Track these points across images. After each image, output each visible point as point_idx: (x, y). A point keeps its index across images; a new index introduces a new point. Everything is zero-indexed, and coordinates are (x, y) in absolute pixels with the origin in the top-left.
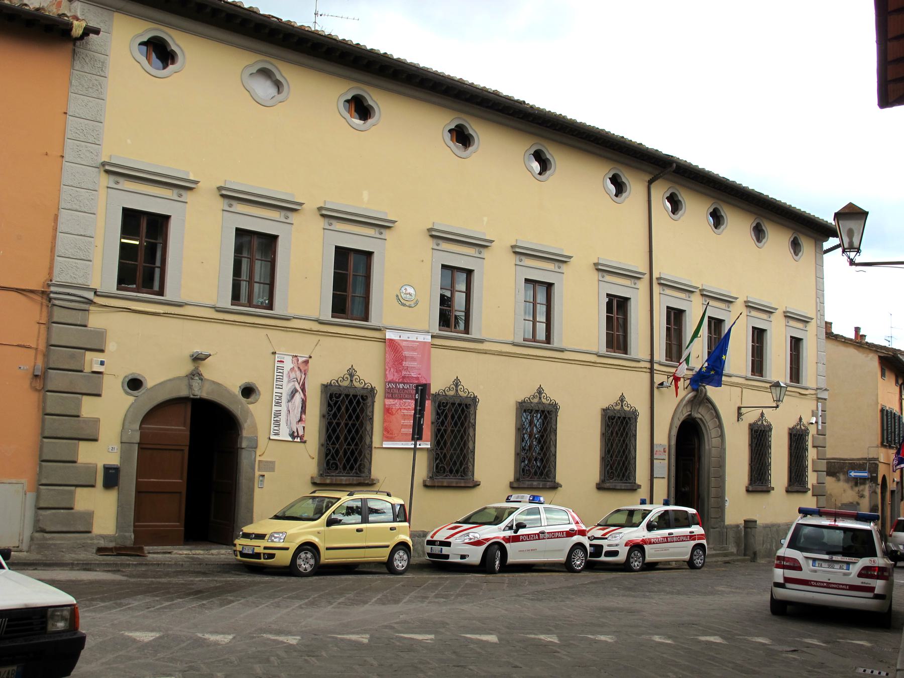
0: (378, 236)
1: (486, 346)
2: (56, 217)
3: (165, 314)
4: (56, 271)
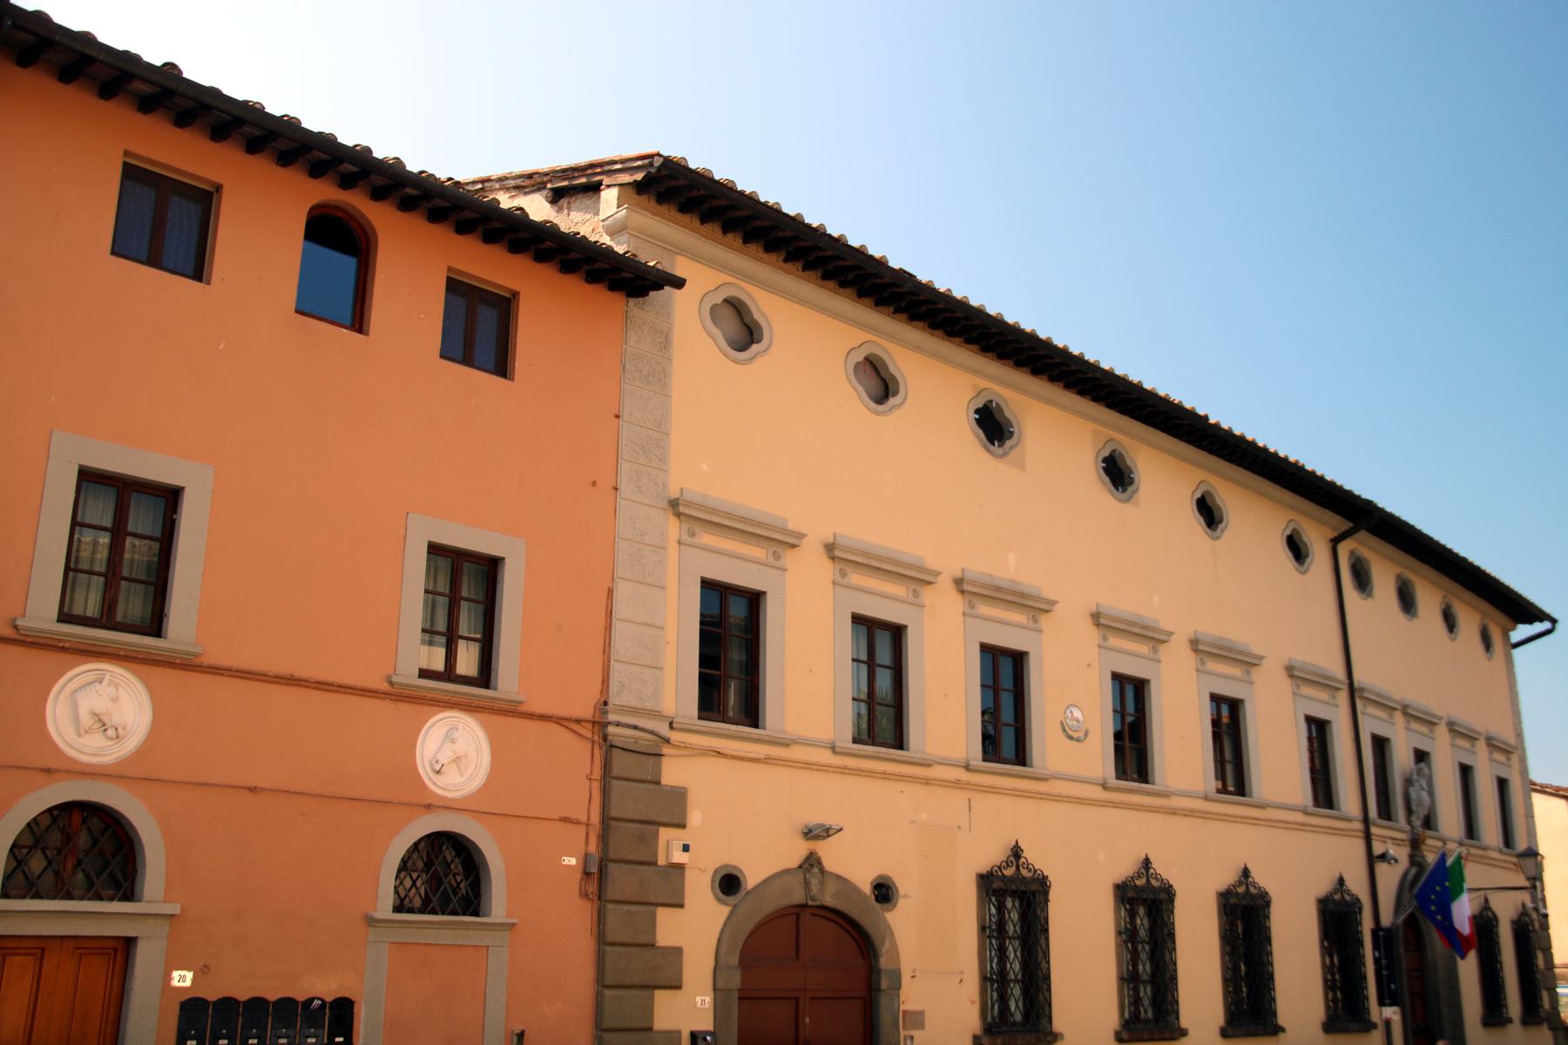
0: (1031, 624)
1: (1175, 802)
2: (610, 592)
3: (767, 760)
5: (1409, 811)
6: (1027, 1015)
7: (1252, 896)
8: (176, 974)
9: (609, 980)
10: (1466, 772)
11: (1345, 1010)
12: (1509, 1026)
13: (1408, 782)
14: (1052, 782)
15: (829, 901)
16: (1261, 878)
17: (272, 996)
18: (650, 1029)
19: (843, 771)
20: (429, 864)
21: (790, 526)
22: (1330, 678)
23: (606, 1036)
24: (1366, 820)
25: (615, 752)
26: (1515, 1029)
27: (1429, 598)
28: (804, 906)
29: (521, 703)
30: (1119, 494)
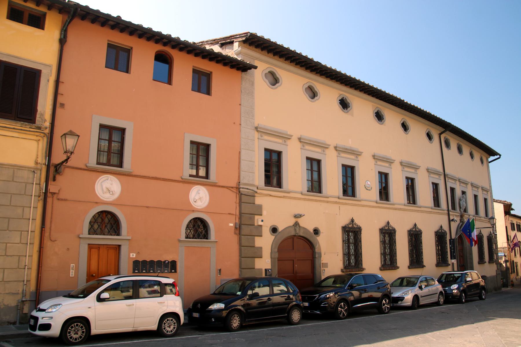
1: (396, 206)
2: (240, 152)
4: (241, 178)
5: (460, 208)
6: (356, 263)
8: (131, 254)
9: (242, 256)
10: (476, 197)
13: (460, 200)
15: (302, 234)
16: (419, 226)
17: (156, 260)
19: (305, 199)
20: (194, 226)
21: (289, 133)
23: (242, 270)
24: (448, 210)
27: (466, 149)
28: (295, 236)
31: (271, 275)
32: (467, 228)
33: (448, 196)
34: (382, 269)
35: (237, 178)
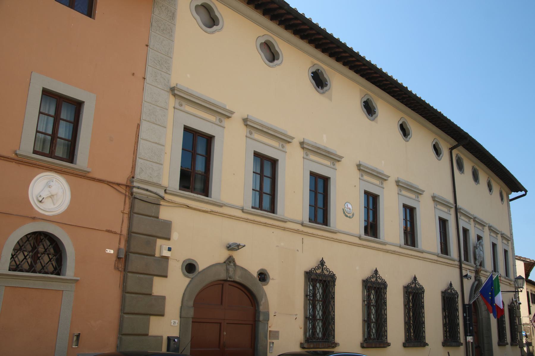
0: (332, 166)
1: (388, 247)
2: (139, 126)
3: (211, 212)
4: (138, 170)
5: (475, 259)
6: (324, 335)
7: (417, 289)
9: (126, 310)
10: (494, 245)
11: (450, 338)
12: (507, 346)
13: (475, 247)
14: (339, 234)
15: (237, 279)
16: (421, 281)
18: (147, 335)
19: (247, 220)
20: (34, 248)
21: (227, 108)
22: (448, 203)
23: (124, 337)
24: (460, 261)
25: (136, 200)
26: (508, 347)
27: (483, 177)
28: (226, 281)
29: (89, 172)
30: (369, 117)
31: (177, 349)
32: (489, 290)
33: (461, 241)
34: (365, 345)
35: (130, 169)
